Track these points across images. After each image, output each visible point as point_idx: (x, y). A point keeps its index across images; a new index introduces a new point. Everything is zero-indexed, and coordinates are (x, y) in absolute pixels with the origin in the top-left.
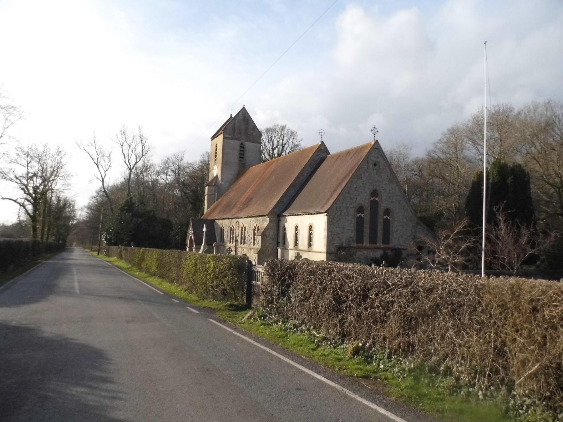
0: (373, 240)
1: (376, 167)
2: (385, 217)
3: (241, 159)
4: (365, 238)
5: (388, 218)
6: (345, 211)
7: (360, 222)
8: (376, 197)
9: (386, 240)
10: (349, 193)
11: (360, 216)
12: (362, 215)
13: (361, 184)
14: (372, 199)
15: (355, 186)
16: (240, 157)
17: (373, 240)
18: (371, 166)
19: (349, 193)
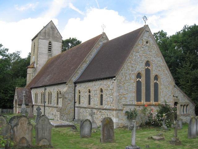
0: (148, 99)
1: (148, 44)
3: (50, 52)
4: (142, 97)
5: (157, 82)
6: (128, 76)
7: (139, 84)
8: (149, 66)
9: (156, 99)
11: (139, 80)
12: (140, 80)
13: (139, 56)
14: (146, 68)
16: (49, 50)
17: (148, 99)
18: (145, 43)
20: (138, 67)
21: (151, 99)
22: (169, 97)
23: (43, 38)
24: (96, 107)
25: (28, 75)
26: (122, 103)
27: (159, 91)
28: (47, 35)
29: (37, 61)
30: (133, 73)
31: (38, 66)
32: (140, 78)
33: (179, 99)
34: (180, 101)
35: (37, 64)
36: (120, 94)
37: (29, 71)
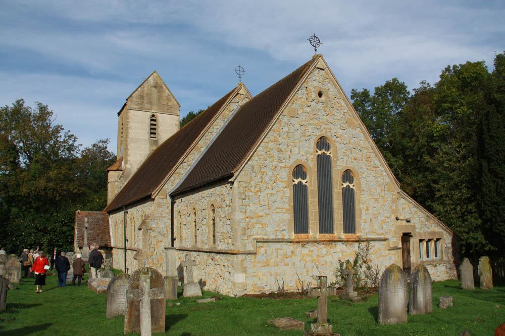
1: (323, 98)
2: (345, 185)
4: (310, 222)
5: (351, 186)
7: (300, 193)
9: (350, 225)
10: (275, 141)
11: (300, 183)
12: (304, 182)
13: (297, 126)
14: (320, 153)
15: (286, 129)
16: (151, 133)
18: (314, 95)
19: (275, 141)
20: (296, 150)
21: (335, 226)
22: (384, 222)
23: (137, 107)
24: (206, 247)
25: (109, 186)
26: (255, 237)
27: (357, 207)
28: (145, 101)
29: (127, 155)
30: (282, 165)
31: (128, 166)
32: (304, 178)
33: (414, 226)
34: (417, 230)
35: (126, 163)
36: (247, 215)
37: (113, 176)
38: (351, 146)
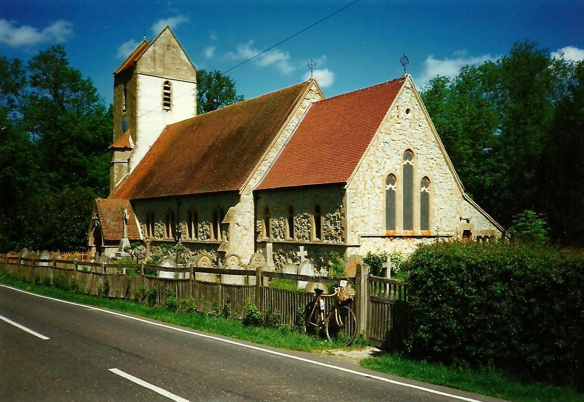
0: (408, 224)
2: (423, 189)
7: (390, 195)
9: (425, 224)
12: (393, 187)
14: (405, 163)
17: (408, 224)
18: (403, 114)
38: (428, 156)
